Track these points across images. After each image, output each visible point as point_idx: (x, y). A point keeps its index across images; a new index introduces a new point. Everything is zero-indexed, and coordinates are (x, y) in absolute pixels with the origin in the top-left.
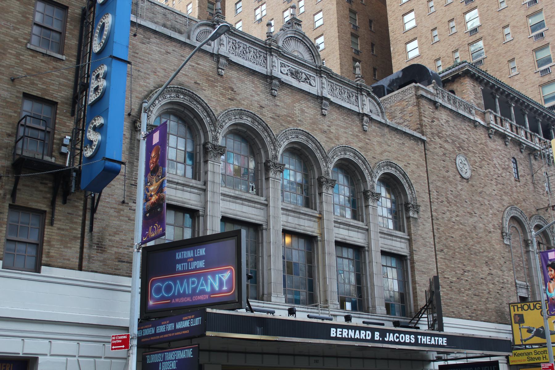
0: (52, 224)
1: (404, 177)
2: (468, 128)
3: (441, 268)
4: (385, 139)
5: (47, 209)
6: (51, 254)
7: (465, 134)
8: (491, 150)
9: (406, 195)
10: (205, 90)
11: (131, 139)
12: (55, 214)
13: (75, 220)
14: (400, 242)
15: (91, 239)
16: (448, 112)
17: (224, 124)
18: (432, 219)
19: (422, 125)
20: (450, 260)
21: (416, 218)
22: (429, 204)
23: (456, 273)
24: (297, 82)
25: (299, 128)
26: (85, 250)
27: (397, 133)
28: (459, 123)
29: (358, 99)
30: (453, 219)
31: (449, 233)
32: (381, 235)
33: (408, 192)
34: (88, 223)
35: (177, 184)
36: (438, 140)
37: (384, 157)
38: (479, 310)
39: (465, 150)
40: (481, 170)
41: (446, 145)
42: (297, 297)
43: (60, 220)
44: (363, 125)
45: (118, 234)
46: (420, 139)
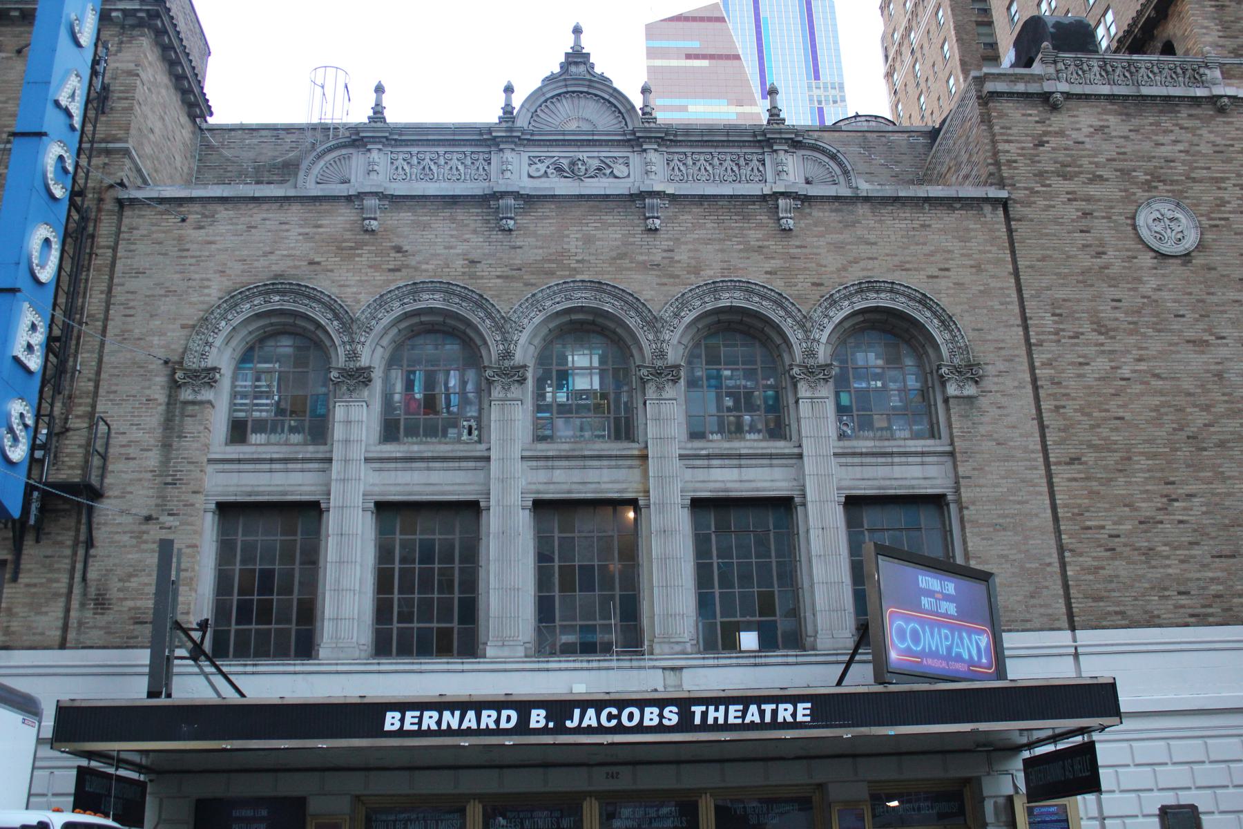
0: (15, 579)
1: (925, 305)
2: (1186, 123)
3: (1066, 506)
4: (858, 233)
5: (9, 557)
6: (12, 629)
7: (1176, 142)
9: (936, 347)
10: (331, 271)
11: (168, 404)
12: (22, 561)
13: (56, 566)
14: (922, 464)
15: (85, 594)
16: (1103, 103)
17: (374, 322)
18: (1036, 388)
19: (997, 164)
20: (1111, 480)
21: (969, 397)
22: (1023, 351)
23: (1136, 509)
24: (576, 183)
25: (579, 278)
26: (73, 614)
27: (904, 204)
28: (1151, 120)
29: (764, 164)
30: (1125, 371)
31: (1107, 411)
32: (843, 460)
33: (940, 336)
34: (79, 566)
35: (272, 461)
36: (1058, 184)
37: (855, 275)
38: (1233, 596)
39: (1172, 182)
41: (1093, 190)
42: (589, 638)
43: (30, 570)
44: (779, 219)
45: (136, 576)
46: (987, 200)
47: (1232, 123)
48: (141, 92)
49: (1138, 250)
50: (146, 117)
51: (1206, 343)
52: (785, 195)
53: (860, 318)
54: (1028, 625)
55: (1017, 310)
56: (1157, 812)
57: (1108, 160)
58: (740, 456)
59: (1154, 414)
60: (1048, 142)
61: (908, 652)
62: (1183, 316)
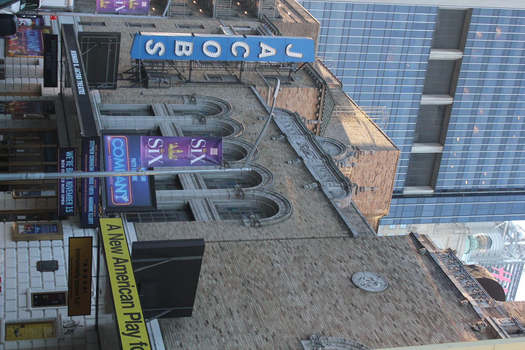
8: (451, 330)
22: (273, 237)
30: (276, 265)
37: (292, 201)
40: (394, 308)
47: (455, 308)
48: (294, 90)
49: (350, 273)
50: (287, 98)
51: (306, 290)
52: (318, 183)
53: (272, 207)
54: (139, 234)
55: (296, 237)
56: (55, 259)
57: (399, 266)
58: (198, 181)
59: (257, 271)
60: (396, 249)
61: (112, 148)
62: (318, 283)
